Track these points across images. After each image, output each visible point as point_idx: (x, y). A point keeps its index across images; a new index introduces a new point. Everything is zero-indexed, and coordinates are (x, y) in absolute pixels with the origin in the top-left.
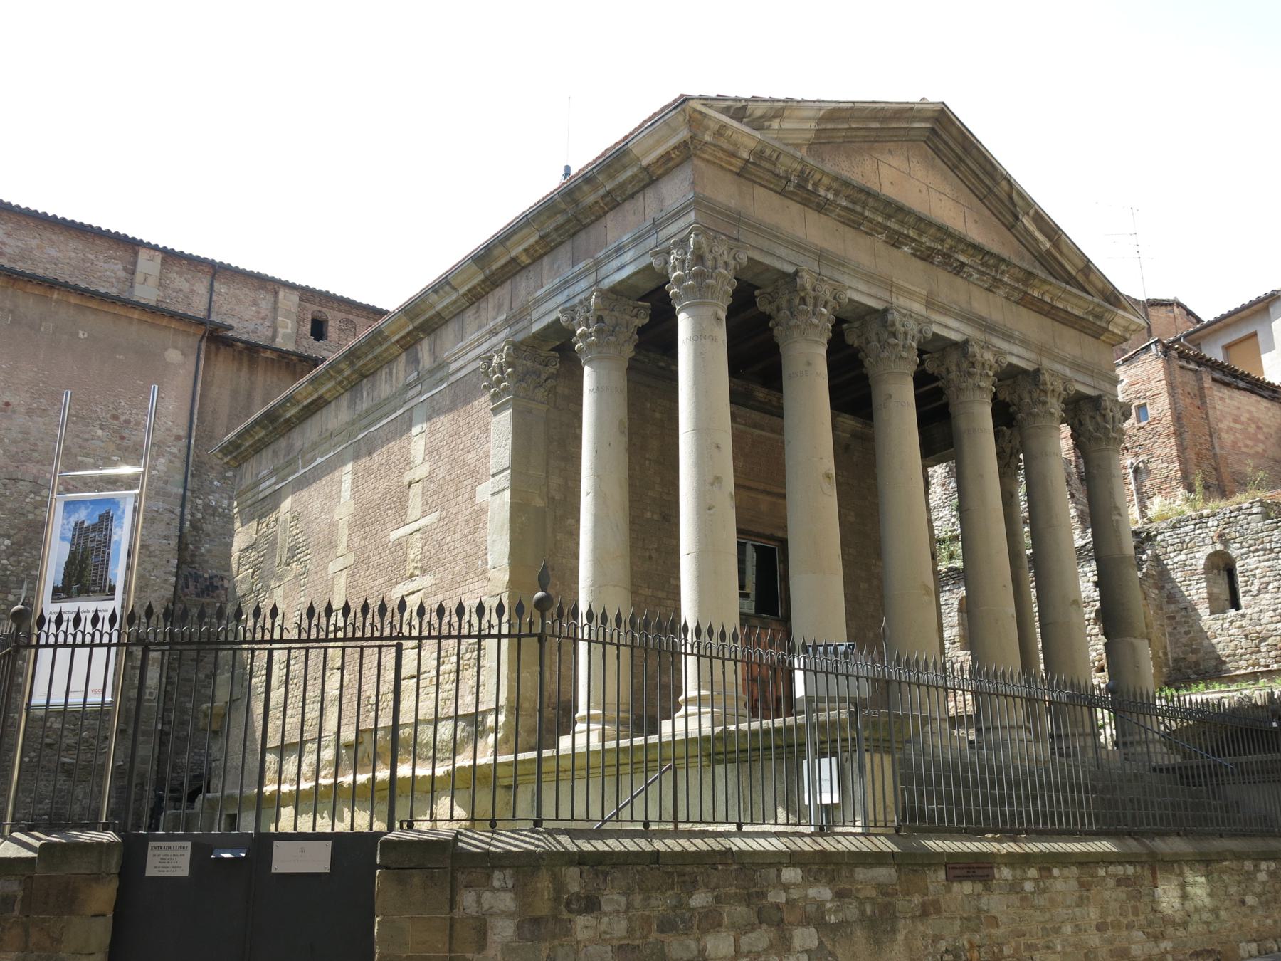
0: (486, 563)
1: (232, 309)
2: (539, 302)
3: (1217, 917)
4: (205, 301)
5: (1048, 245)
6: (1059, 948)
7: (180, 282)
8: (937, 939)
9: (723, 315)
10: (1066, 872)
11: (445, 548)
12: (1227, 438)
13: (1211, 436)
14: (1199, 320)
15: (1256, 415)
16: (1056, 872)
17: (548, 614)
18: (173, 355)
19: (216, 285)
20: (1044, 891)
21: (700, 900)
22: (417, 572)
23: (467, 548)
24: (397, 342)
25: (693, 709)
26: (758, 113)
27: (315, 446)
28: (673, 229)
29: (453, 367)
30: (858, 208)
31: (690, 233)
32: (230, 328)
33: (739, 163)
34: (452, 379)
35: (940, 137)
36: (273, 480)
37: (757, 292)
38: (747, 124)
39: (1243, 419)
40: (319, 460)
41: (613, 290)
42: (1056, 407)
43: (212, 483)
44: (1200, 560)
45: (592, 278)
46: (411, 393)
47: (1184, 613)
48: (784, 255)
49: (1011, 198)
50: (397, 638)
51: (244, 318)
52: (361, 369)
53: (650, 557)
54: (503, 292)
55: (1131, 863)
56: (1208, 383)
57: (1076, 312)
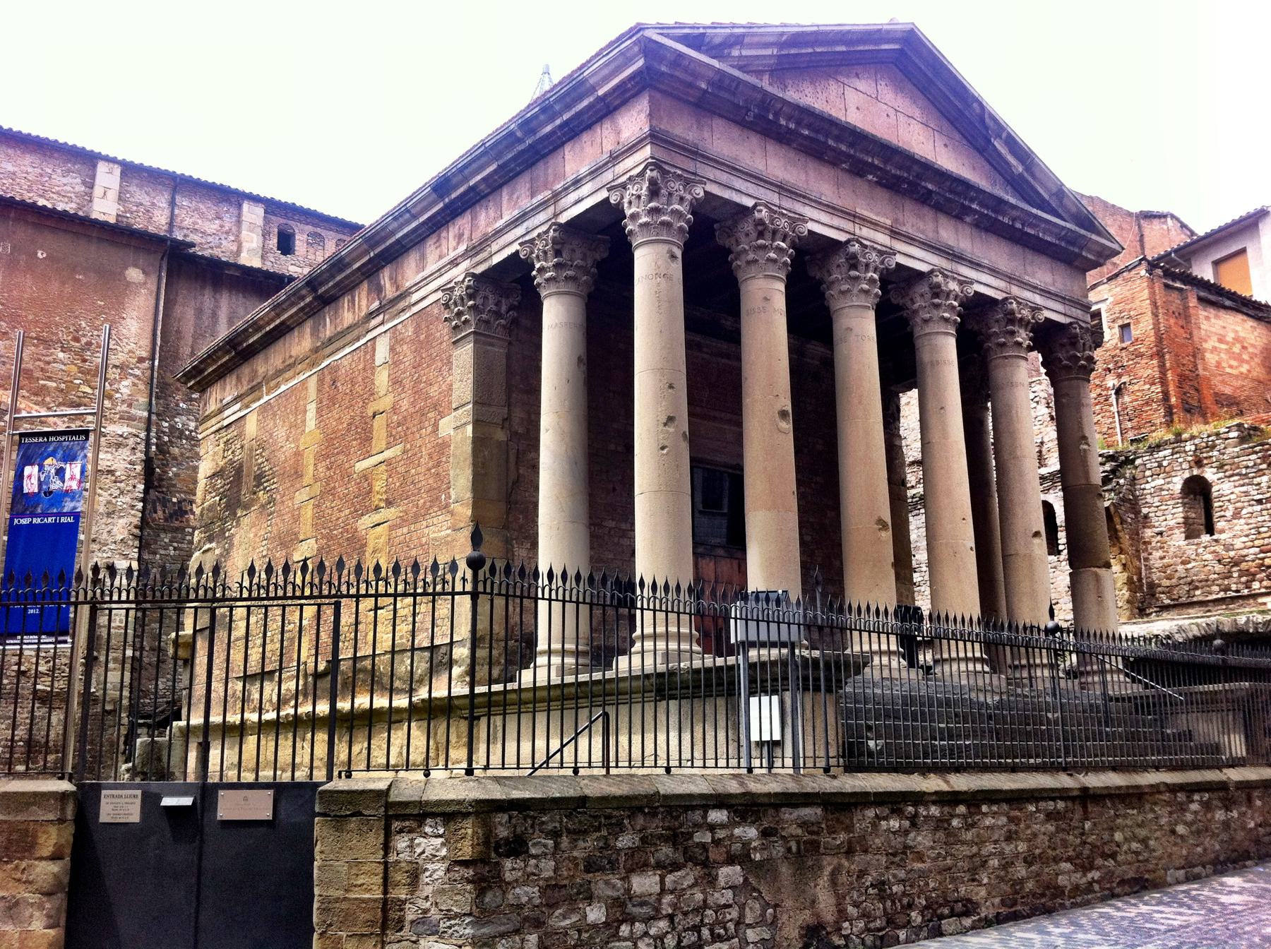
0: (450, 498)
1: (195, 223)
2: (499, 233)
3: (1147, 846)
4: (167, 212)
5: (1020, 169)
6: (985, 881)
7: (140, 195)
8: (862, 874)
9: (679, 253)
10: (995, 808)
11: (410, 480)
12: (1211, 358)
13: (1194, 356)
14: (1192, 233)
15: (1242, 334)
16: (984, 808)
17: (481, 572)
18: (134, 274)
19: (178, 199)
20: (973, 825)
21: (625, 841)
22: (383, 504)
23: (431, 481)
24: (358, 268)
25: (649, 645)
26: (717, 41)
27: (279, 373)
28: (629, 163)
29: (415, 297)
30: (821, 138)
31: (646, 168)
32: (192, 245)
33: (697, 94)
34: (415, 309)
35: (907, 61)
36: (238, 406)
37: (716, 226)
38: (707, 53)
39: (1229, 338)
40: (283, 388)
41: (572, 223)
42: (1023, 336)
43: (177, 405)
44: (1177, 484)
45: (551, 210)
46: (374, 323)
47: (1159, 538)
48: (743, 189)
49: (982, 121)
50: (334, 596)
51: (205, 231)
52: (323, 293)
53: (614, 489)
54: (463, 222)
55: (1062, 799)
56: (1193, 302)
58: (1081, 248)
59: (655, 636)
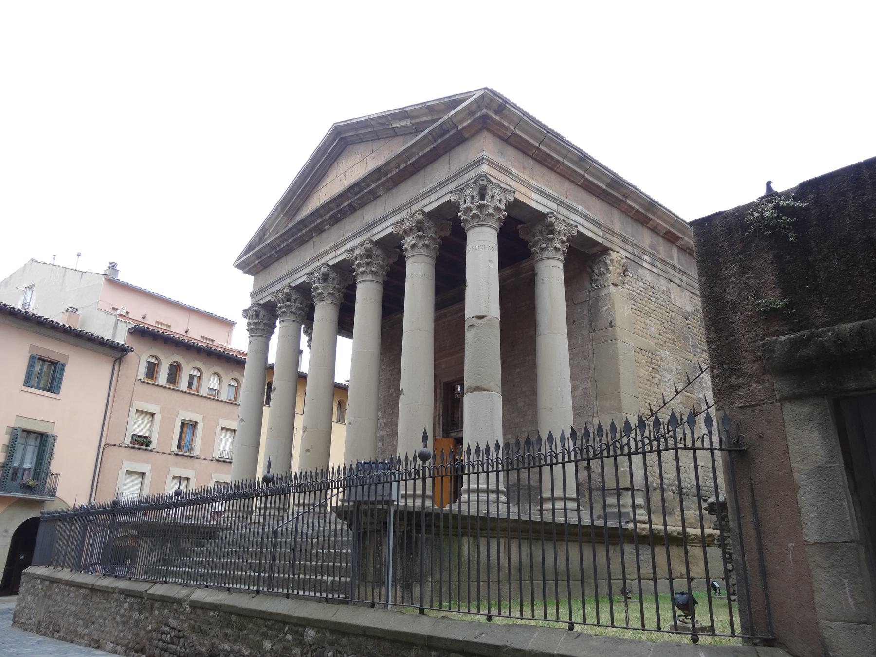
26: (257, 240)
35: (342, 140)
57: (427, 150)
58: (456, 126)
59: (478, 491)
